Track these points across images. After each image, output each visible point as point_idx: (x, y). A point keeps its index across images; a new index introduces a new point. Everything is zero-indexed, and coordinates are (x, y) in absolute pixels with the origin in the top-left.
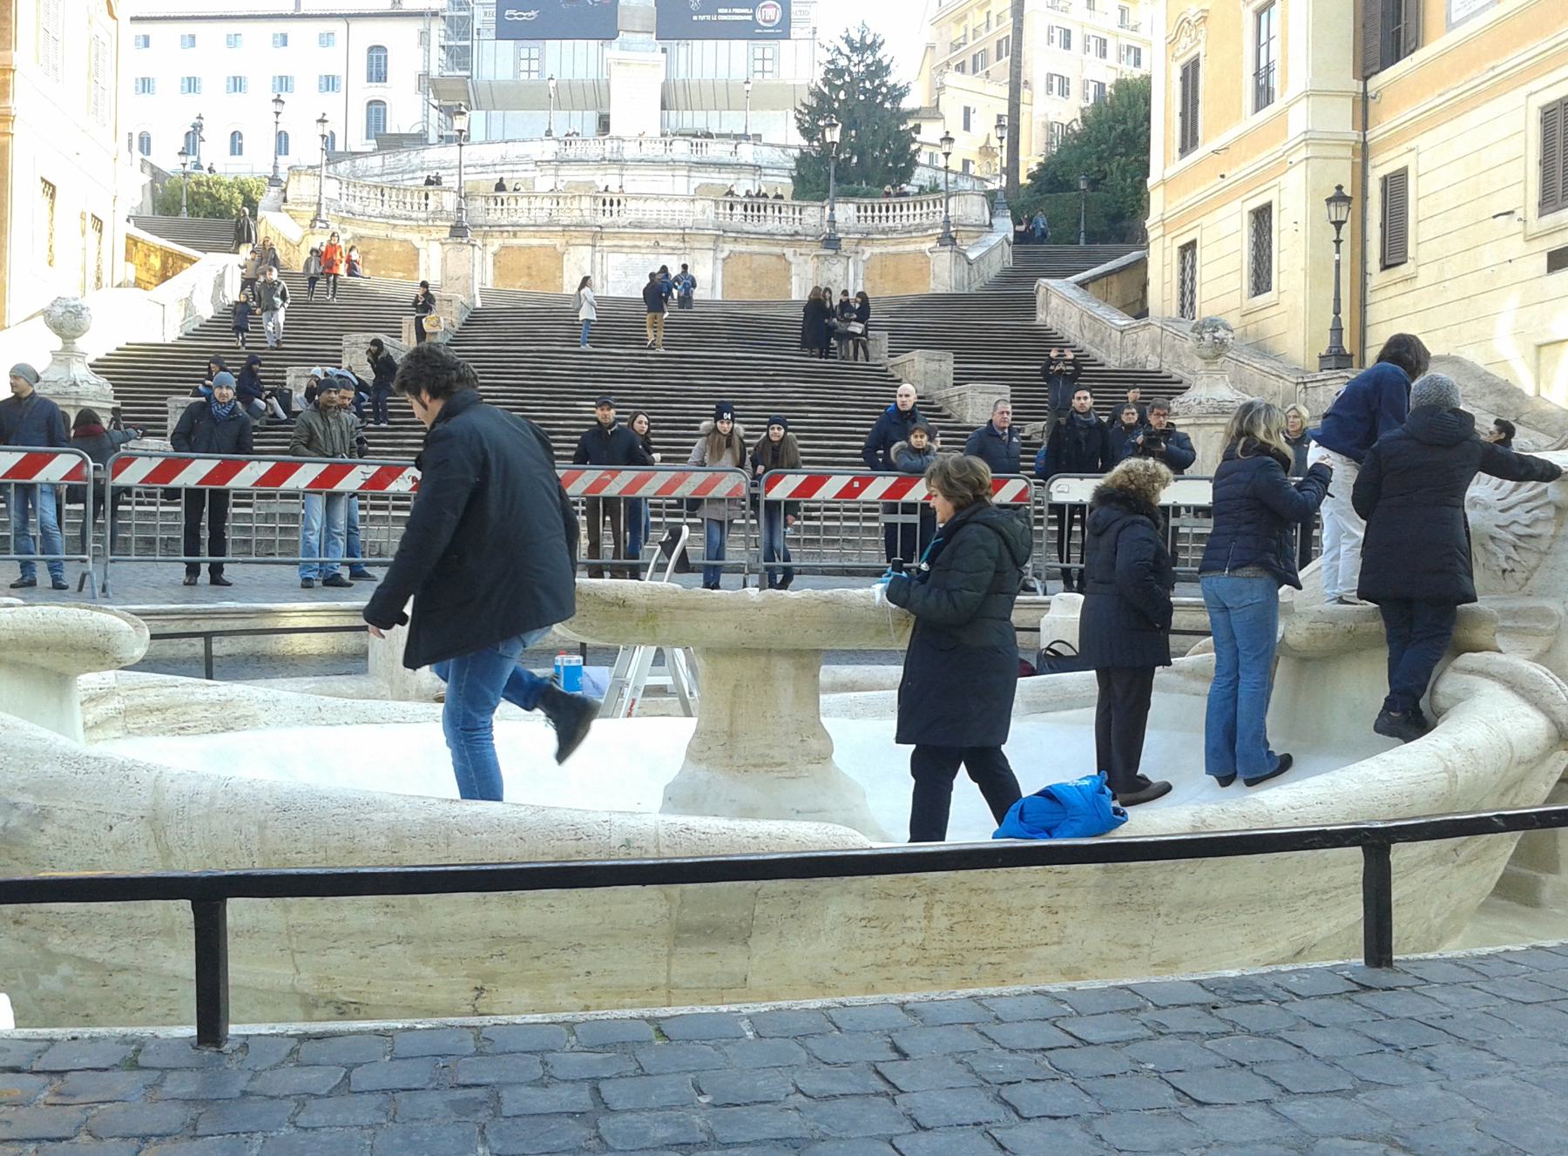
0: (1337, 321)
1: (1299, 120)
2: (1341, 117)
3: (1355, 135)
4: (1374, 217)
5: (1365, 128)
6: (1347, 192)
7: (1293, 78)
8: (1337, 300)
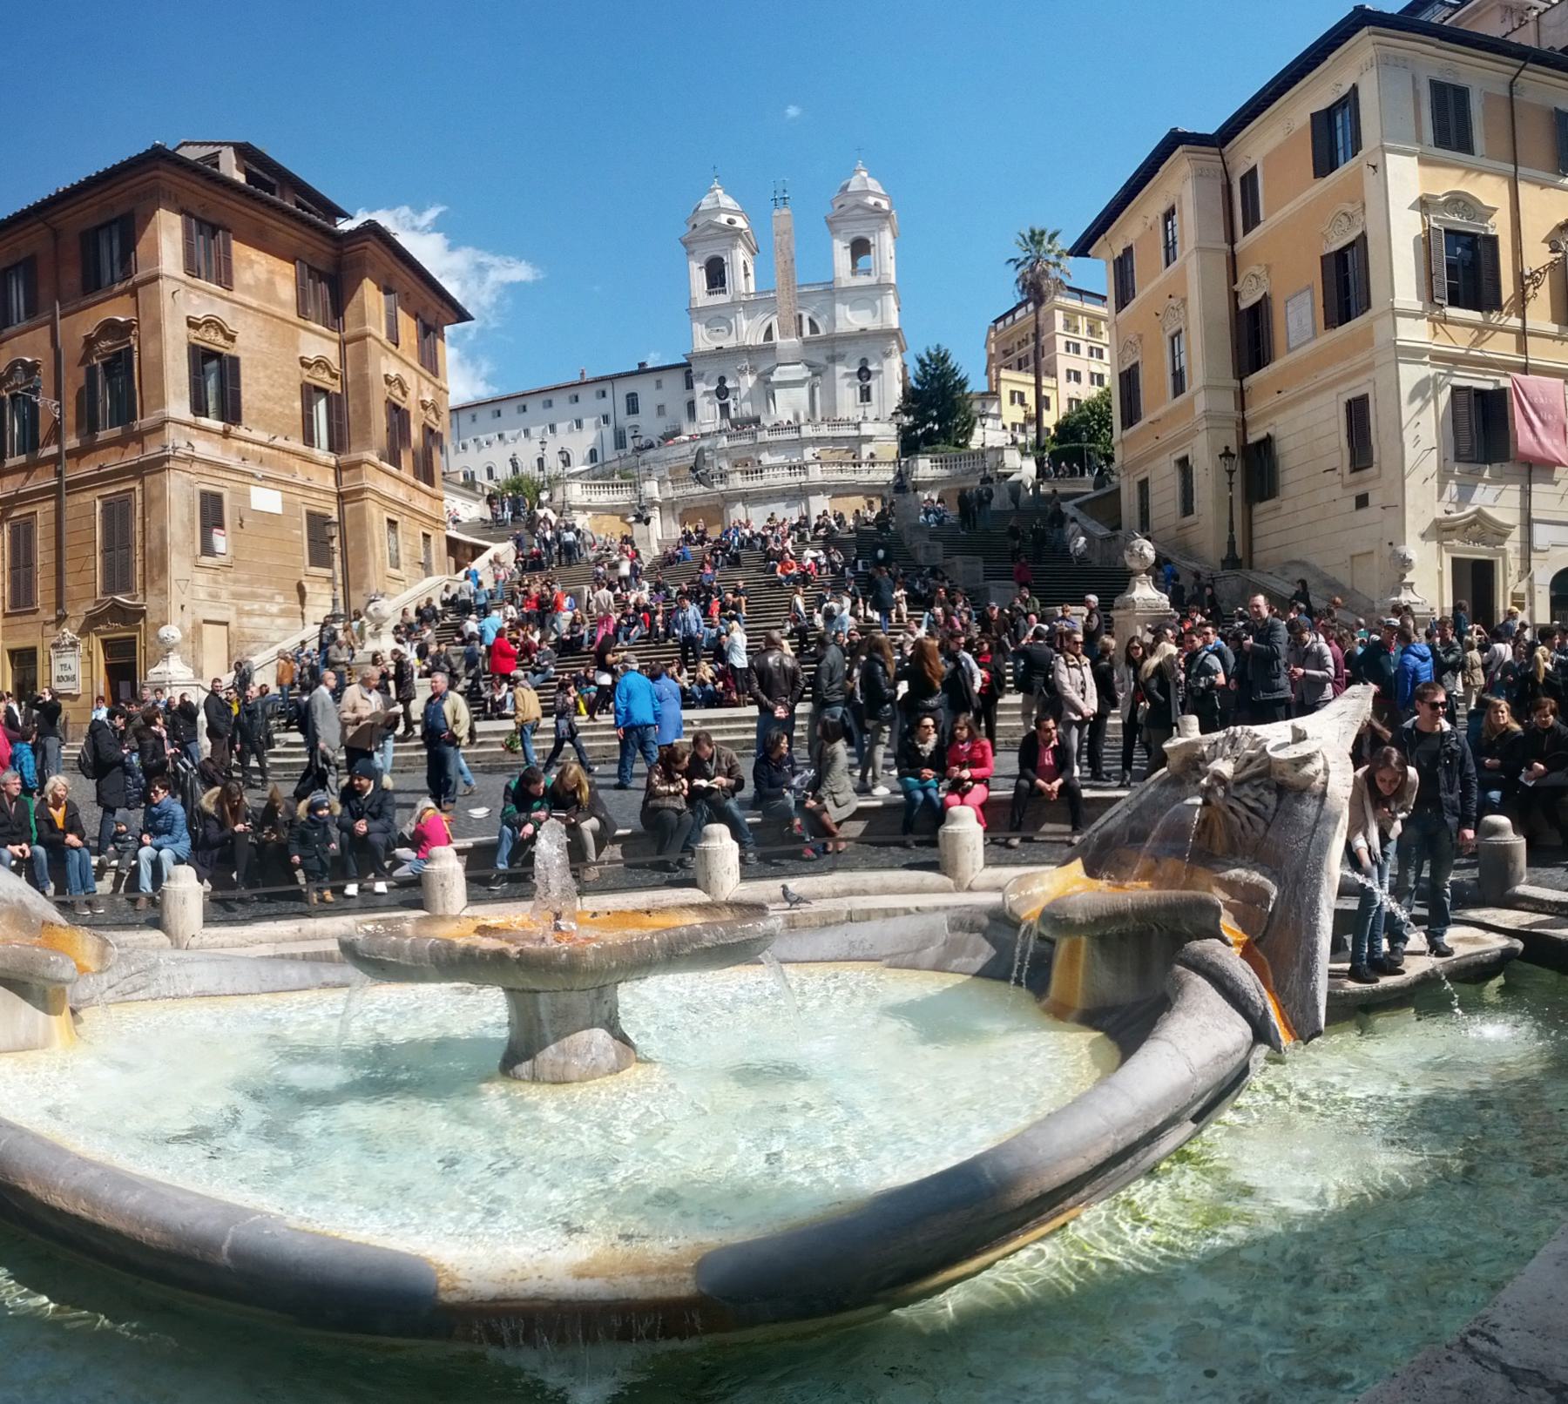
0: (1232, 537)
1: (1201, 404)
2: (1228, 403)
3: (1238, 414)
4: (1256, 467)
5: (1243, 409)
6: (1234, 450)
7: (1196, 378)
8: (1231, 522)
